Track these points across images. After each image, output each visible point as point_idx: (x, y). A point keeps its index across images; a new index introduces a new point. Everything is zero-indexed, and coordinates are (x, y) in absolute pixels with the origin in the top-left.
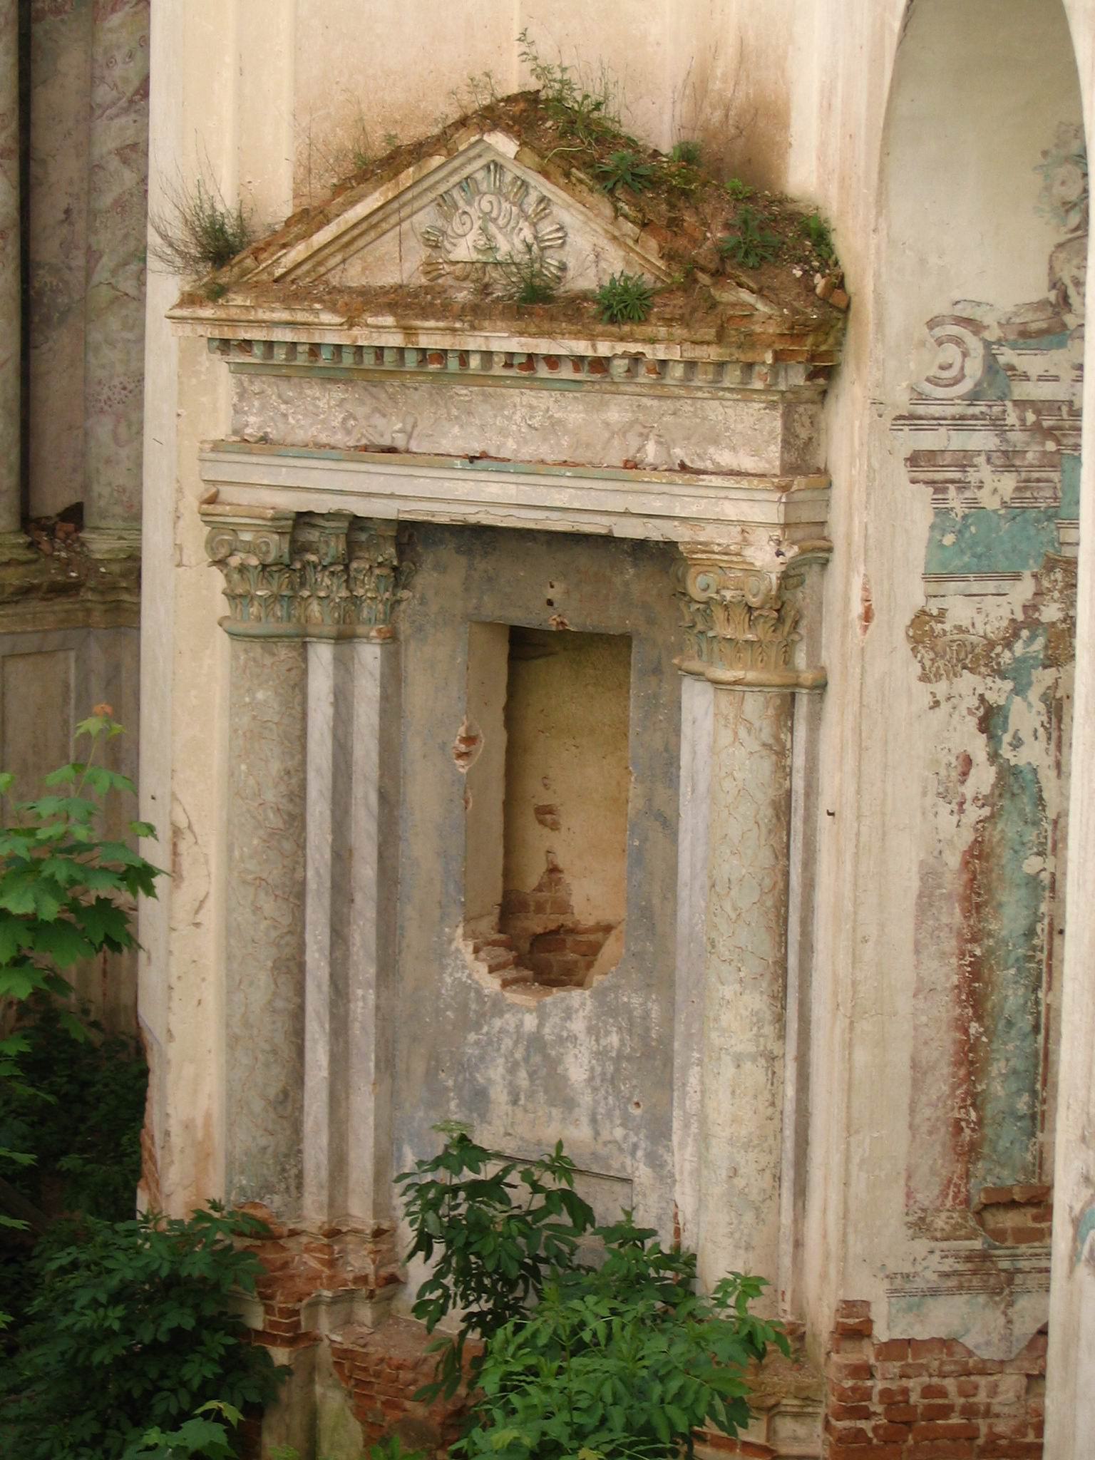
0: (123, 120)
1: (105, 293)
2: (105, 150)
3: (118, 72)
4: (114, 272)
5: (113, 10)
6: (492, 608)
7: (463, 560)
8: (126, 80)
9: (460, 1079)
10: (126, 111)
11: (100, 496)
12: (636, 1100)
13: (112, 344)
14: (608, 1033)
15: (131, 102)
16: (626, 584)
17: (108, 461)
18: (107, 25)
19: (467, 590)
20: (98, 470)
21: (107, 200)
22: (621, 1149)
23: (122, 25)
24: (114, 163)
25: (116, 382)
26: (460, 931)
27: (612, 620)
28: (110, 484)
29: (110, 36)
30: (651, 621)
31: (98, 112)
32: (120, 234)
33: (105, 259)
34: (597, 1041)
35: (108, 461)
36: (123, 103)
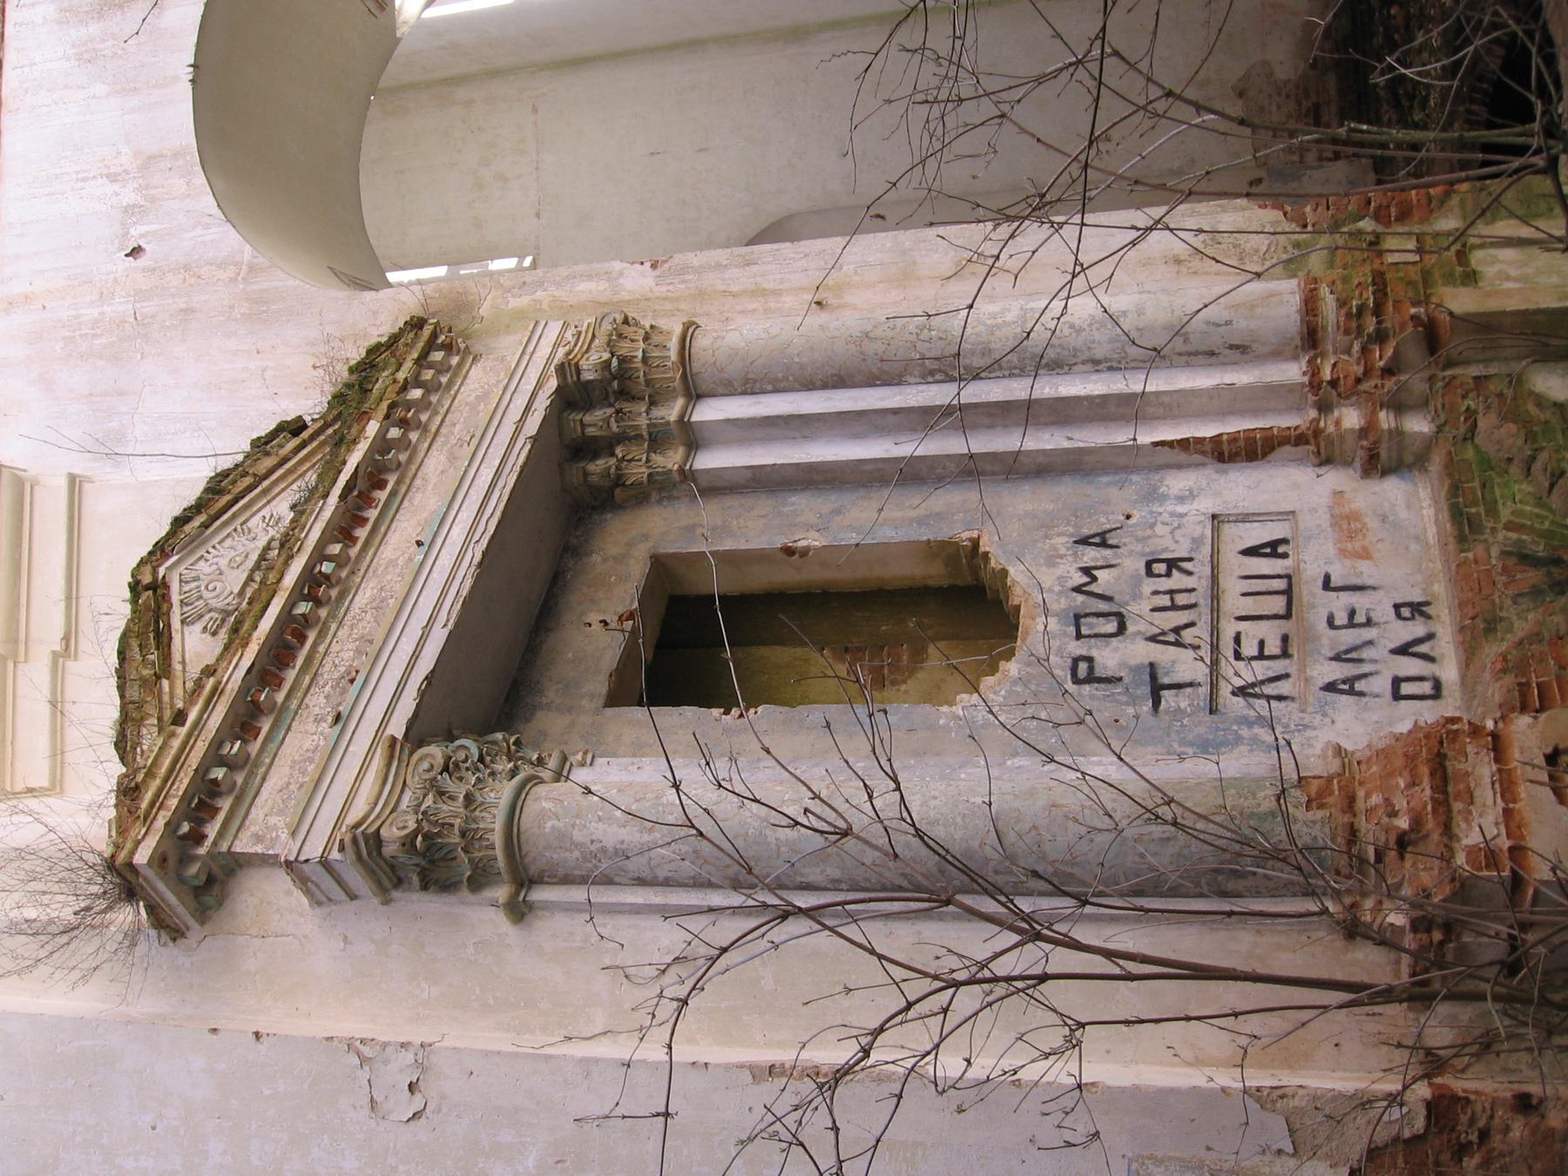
6: (600, 685)
7: (540, 714)
9: (1124, 698)
12: (1122, 518)
14: (1054, 548)
16: (605, 560)
19: (570, 710)
22: (1179, 527)
26: (945, 709)
27: (638, 569)
30: (645, 537)
34: (1062, 557)
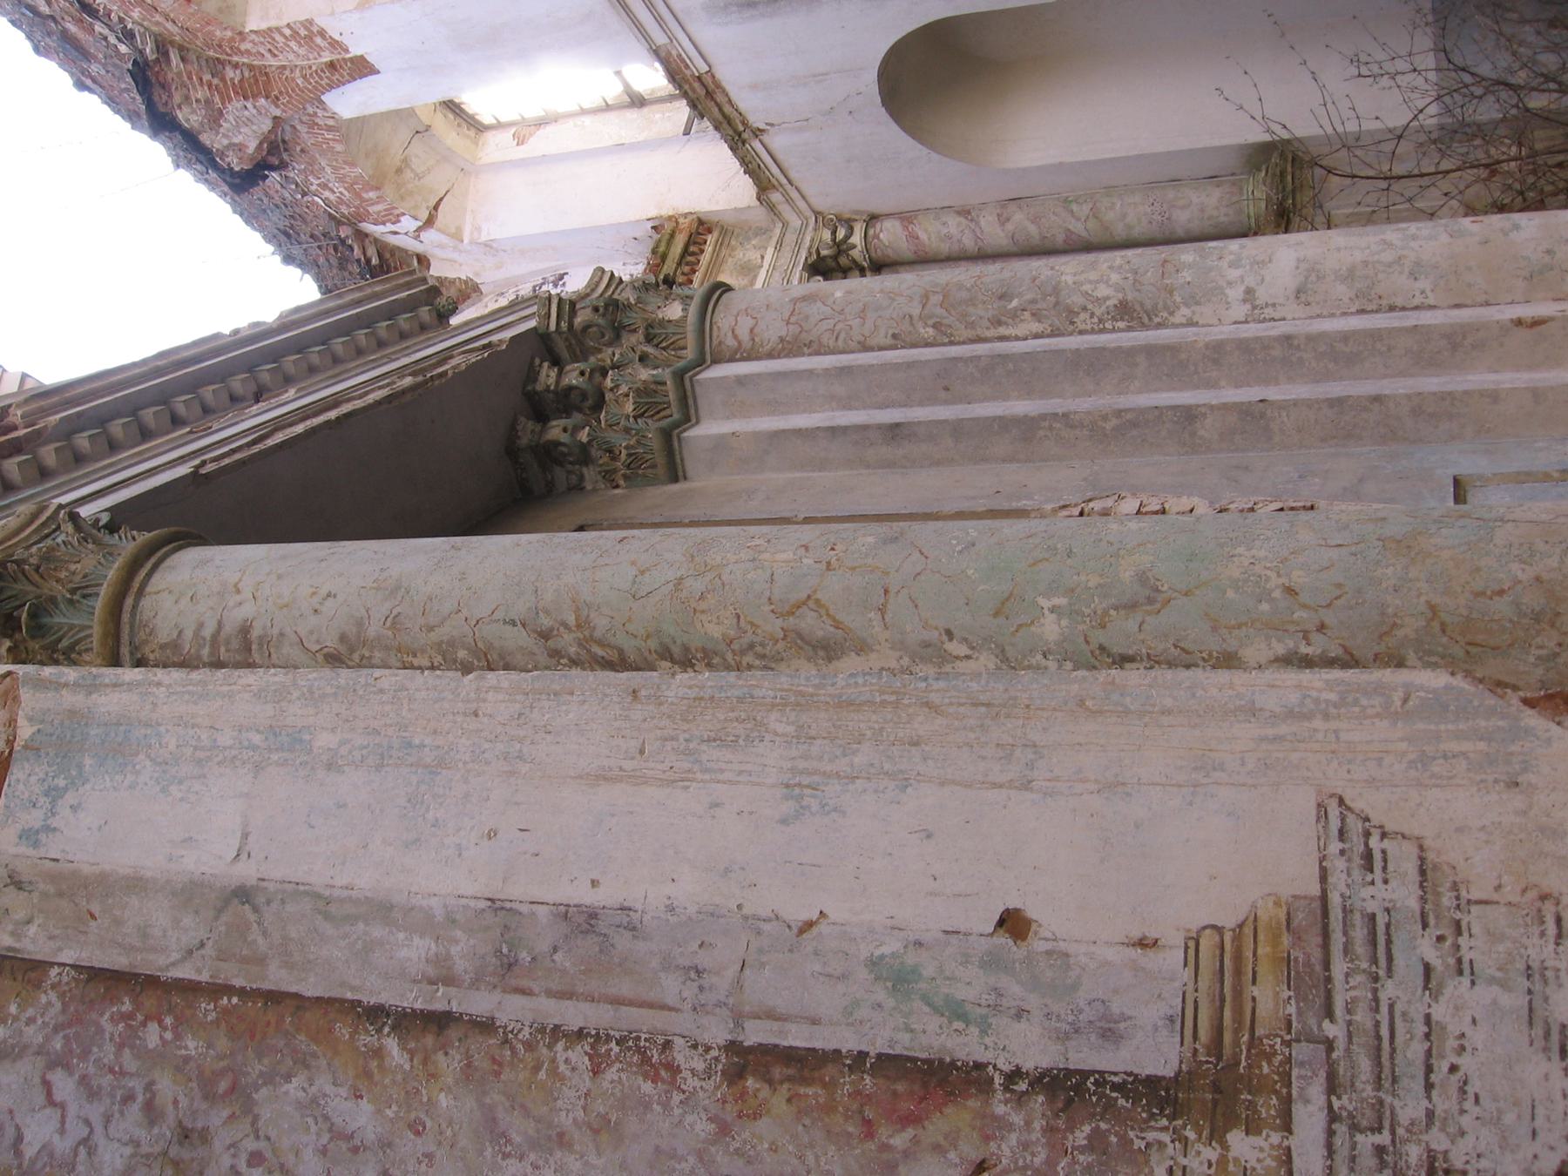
0: (983, 223)
1: (1091, 224)
2: (1002, 234)
3: (953, 230)
4: (1078, 219)
5: (918, 238)
8: (959, 224)
10: (977, 223)
11: (1226, 215)
13: (1124, 216)
15: (972, 220)
17: (1202, 210)
18: (927, 242)
20: (1209, 218)
21: (1033, 229)
23: (926, 230)
24: (1010, 227)
25: (1149, 210)
28: (1217, 208)
29: (933, 239)
31: (980, 243)
32: (1053, 218)
33: (1071, 227)
35: (1202, 210)
36: (972, 225)
